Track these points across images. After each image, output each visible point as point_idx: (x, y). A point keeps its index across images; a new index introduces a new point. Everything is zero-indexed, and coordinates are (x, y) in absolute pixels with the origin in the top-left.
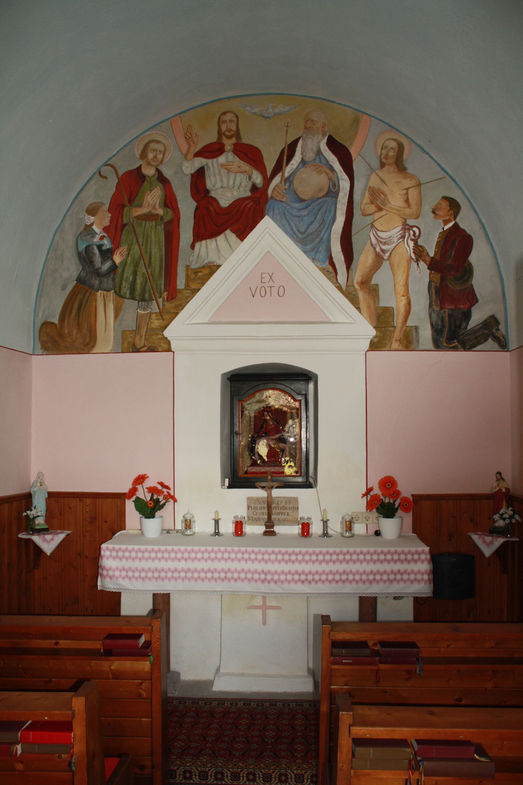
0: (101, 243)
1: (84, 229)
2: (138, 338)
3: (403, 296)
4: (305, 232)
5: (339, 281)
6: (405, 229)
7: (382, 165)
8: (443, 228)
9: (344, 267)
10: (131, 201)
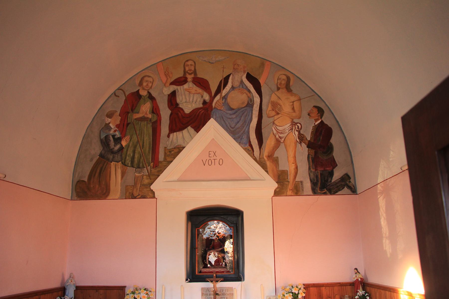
0: (114, 134)
2: (135, 190)
3: (293, 163)
6: (293, 125)
7: (278, 89)
10: (132, 110)
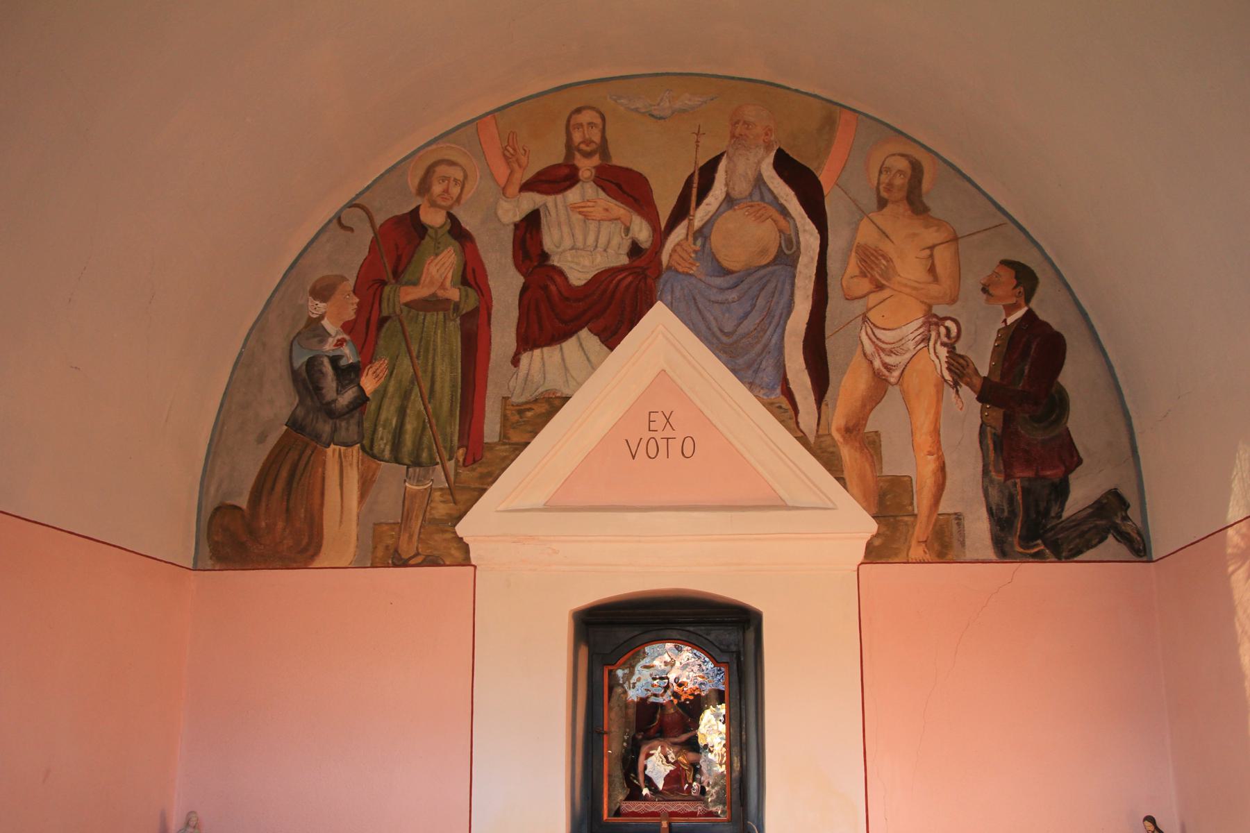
0: (338, 353)
1: (306, 327)
2: (404, 537)
3: (930, 454)
5: (802, 426)
7: (882, 203)
8: (1005, 321)
9: (812, 398)
10: (397, 274)
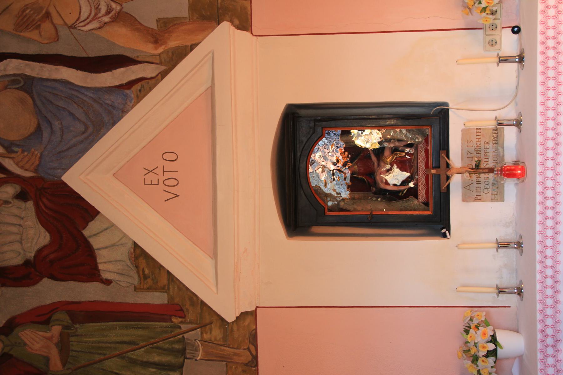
2: (236, 359)
4: (84, 123)
5: (154, 75)
9: (133, 67)
